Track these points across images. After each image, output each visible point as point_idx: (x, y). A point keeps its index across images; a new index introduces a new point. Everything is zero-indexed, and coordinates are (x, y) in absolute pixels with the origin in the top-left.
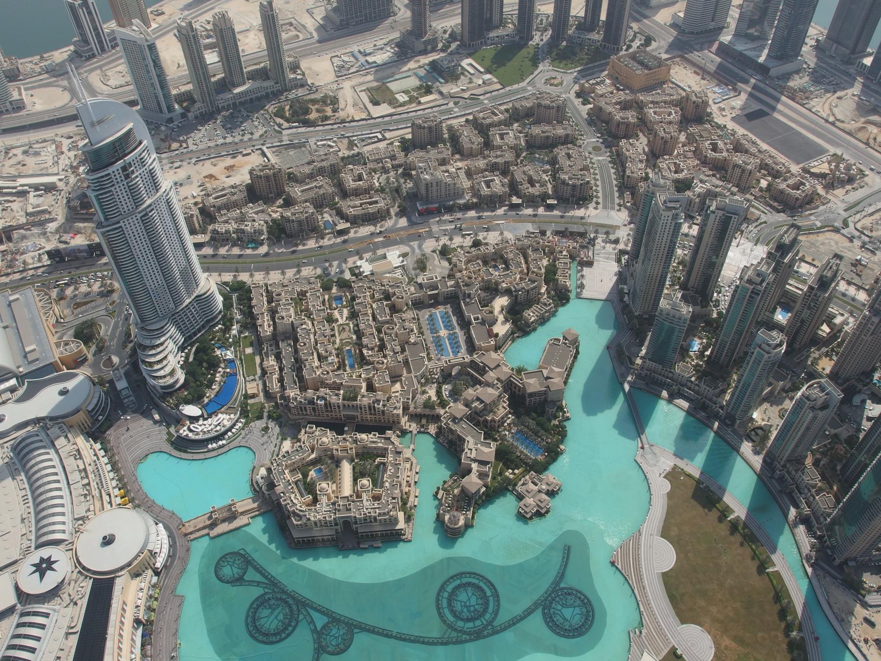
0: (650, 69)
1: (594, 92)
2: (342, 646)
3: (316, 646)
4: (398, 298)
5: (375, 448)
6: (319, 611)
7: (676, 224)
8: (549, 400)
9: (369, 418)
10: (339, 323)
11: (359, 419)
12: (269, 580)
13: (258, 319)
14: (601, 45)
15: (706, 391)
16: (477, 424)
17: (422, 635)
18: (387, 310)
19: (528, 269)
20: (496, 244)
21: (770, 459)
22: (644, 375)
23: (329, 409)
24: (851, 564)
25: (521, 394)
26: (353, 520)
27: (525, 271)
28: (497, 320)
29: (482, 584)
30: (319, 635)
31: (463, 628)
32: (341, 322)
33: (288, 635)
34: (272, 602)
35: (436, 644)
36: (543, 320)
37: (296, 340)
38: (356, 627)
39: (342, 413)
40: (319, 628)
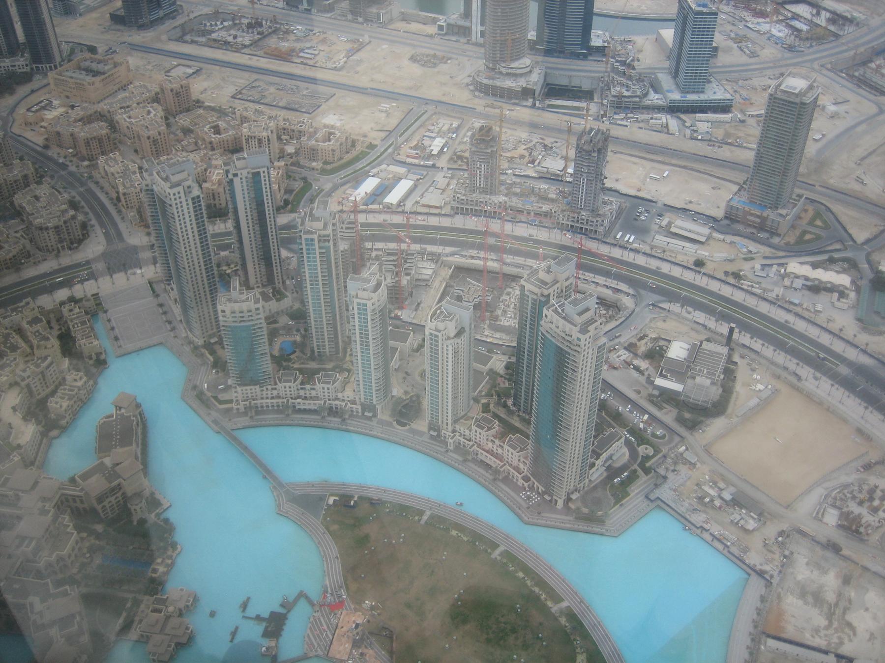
0: (104, 73)
1: (43, 120)
7: (193, 199)
8: (129, 494)
14: (32, 69)
15: (326, 390)
19: (32, 347)
21: (435, 430)
22: (242, 410)
24: (574, 497)
25: (86, 505)
27: (28, 350)
36: (82, 402)
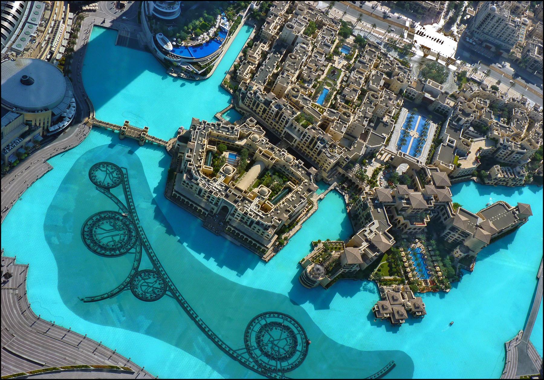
2: (148, 295)
3: (128, 280)
4: (398, 79)
5: (292, 173)
6: (151, 258)
9: (303, 149)
10: (334, 65)
11: (295, 145)
12: (129, 206)
13: (270, 17)
16: (391, 218)
17: (220, 336)
18: (382, 82)
20: (513, 100)
23: (277, 119)
26: (232, 212)
28: (468, 155)
29: (299, 337)
30: (136, 273)
31: (258, 357)
32: (336, 65)
33: (112, 256)
34: (119, 223)
35: (227, 353)
37: (290, 51)
38: (171, 290)
39: (286, 129)
40: (140, 269)
